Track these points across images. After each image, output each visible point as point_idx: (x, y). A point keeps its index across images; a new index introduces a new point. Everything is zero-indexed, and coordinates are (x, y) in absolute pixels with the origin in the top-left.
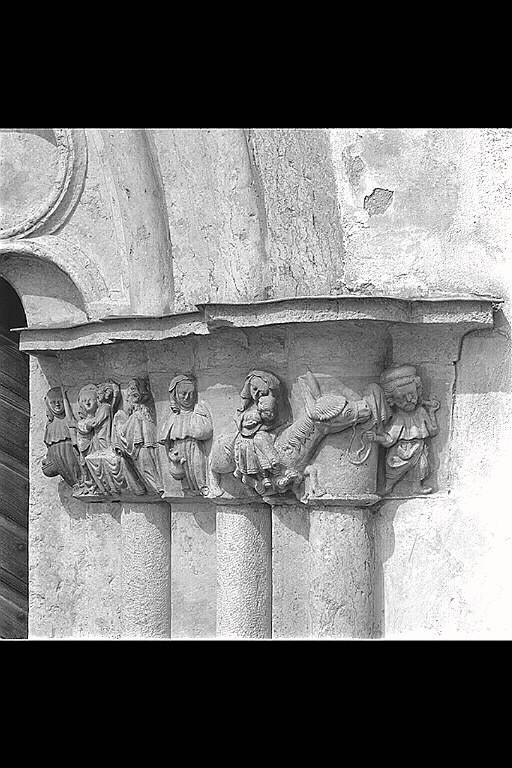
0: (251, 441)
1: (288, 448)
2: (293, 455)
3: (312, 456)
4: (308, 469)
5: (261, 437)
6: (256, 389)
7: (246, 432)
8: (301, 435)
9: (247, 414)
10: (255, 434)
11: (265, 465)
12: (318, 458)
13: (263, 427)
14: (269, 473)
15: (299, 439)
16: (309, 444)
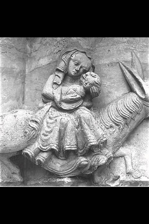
0: (72, 117)
1: (111, 127)
2: (115, 135)
3: (127, 139)
4: (123, 151)
5: (85, 113)
6: (77, 64)
7: (65, 106)
8: (127, 114)
9: (65, 89)
10: (77, 109)
11: (93, 140)
12: (134, 140)
13: (85, 104)
14: (90, 151)
15: (124, 118)
16: (132, 125)
